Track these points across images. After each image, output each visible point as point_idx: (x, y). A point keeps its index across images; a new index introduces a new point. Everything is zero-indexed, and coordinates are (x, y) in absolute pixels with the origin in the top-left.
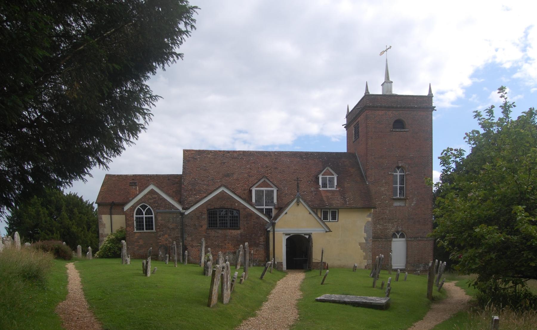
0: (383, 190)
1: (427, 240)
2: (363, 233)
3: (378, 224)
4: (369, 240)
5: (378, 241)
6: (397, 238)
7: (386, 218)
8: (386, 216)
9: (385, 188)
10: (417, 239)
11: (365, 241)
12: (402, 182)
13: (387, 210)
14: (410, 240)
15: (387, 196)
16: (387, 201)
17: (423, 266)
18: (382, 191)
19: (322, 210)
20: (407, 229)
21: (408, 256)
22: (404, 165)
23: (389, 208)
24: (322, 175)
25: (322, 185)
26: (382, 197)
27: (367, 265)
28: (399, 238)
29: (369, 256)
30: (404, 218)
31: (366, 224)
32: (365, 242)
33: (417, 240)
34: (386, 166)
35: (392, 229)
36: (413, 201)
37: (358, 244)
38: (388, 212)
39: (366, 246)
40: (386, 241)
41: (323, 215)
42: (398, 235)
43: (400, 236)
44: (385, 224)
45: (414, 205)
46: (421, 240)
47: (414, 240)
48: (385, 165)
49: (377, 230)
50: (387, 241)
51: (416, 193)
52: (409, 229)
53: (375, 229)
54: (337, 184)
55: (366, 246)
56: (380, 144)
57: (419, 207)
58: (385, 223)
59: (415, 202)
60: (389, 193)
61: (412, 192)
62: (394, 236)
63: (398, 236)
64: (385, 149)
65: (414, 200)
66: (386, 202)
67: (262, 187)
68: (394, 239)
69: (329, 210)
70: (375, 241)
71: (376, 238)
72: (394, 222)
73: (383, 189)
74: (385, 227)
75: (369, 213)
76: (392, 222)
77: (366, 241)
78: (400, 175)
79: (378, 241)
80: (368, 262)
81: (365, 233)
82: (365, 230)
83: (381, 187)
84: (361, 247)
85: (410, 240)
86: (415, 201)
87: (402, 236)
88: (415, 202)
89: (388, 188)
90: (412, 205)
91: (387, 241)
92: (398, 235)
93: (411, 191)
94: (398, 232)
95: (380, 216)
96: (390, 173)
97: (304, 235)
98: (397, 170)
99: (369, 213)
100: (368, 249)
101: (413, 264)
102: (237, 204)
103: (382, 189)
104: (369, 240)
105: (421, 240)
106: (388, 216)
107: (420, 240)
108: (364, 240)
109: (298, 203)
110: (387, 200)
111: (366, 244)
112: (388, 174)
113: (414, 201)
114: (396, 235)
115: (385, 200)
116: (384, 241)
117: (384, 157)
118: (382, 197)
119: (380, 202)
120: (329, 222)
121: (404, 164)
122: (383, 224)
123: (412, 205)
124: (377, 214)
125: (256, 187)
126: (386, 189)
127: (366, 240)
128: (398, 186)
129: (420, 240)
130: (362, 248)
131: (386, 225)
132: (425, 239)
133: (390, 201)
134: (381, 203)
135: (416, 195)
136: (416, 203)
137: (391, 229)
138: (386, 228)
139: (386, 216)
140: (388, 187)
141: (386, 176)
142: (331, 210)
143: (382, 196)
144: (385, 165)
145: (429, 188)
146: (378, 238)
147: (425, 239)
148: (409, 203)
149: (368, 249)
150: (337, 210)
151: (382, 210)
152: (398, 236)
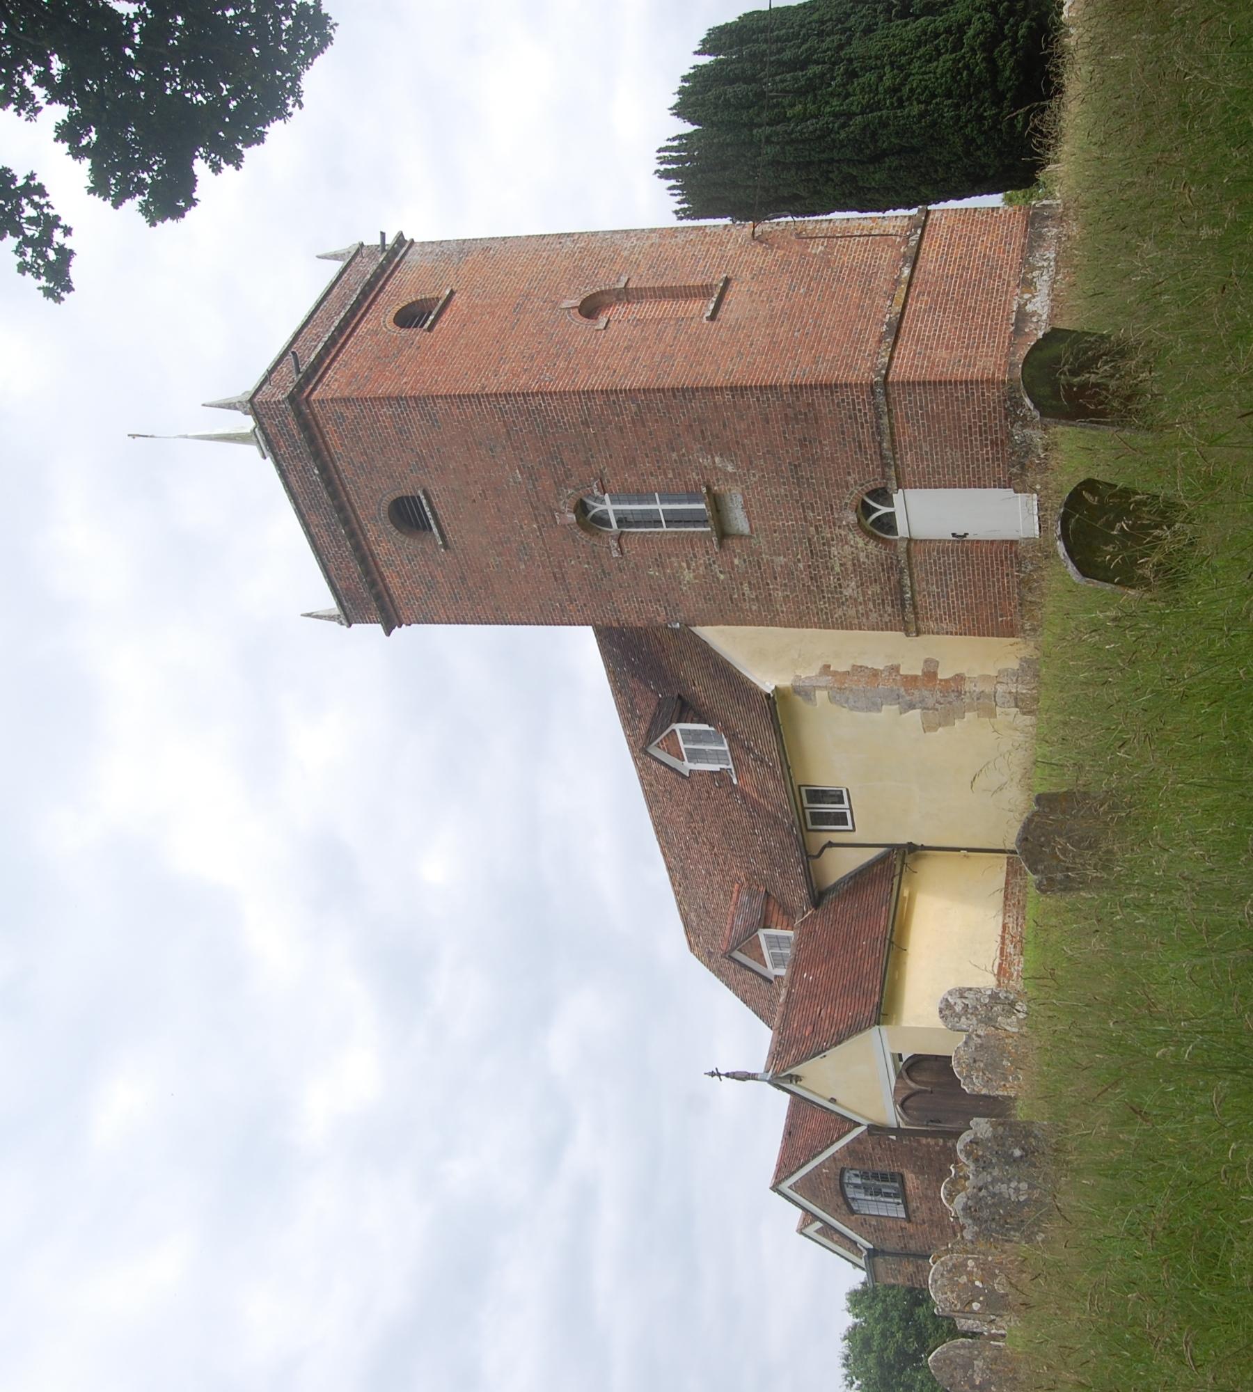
0: (691, 575)
1: (890, 410)
2: (879, 714)
3: (841, 593)
4: (908, 698)
5: (913, 597)
6: (893, 514)
7: (809, 566)
8: (801, 565)
9: (681, 567)
10: (889, 454)
11: (916, 713)
12: (641, 497)
13: (772, 561)
14: (894, 482)
15: (714, 562)
16: (736, 561)
17: (1023, 427)
18: (695, 578)
19: (810, 826)
20: (847, 488)
21: (976, 481)
22: (567, 501)
23: (761, 554)
24: (683, 760)
25: (719, 763)
26: (722, 577)
27: (1017, 706)
28: (893, 506)
29: (981, 701)
30: (797, 501)
31: (846, 705)
32: (918, 711)
33: (895, 453)
34: (588, 563)
35: (852, 543)
36: (715, 468)
37: (927, 733)
38: (782, 557)
39: (937, 710)
40: (910, 570)
41: (827, 824)
42: (878, 510)
43: (882, 505)
44: (837, 569)
45: (732, 461)
46: (892, 434)
47: (896, 466)
48: (586, 566)
49: (864, 596)
50: (909, 564)
51: (674, 455)
52: (847, 482)
53: (861, 604)
54: (705, 723)
55: (937, 710)
56: (511, 582)
57: (738, 443)
58: (832, 569)
59: (717, 459)
60: (699, 556)
61: (673, 470)
62: (887, 524)
63: (884, 510)
64: (523, 567)
65: (707, 462)
66: (737, 566)
67: (762, 955)
68: (902, 530)
69: (807, 812)
70: (915, 607)
71: (903, 606)
72: (823, 538)
73: (688, 576)
74: (851, 568)
75: (799, 699)
76: (824, 544)
77: (915, 709)
78: (613, 502)
79: (913, 597)
80: (1004, 703)
81: (879, 710)
82: (868, 709)
83: (680, 583)
84: (940, 725)
85: (898, 479)
86: (713, 457)
87: (882, 495)
88: (717, 459)
89: (678, 557)
90: (730, 469)
91: (909, 564)
92: (878, 510)
93: (670, 476)
94: (868, 510)
95: (804, 585)
96: (615, 554)
97: (901, 1060)
98: (596, 510)
99: (799, 699)
100: (950, 703)
101: (1014, 470)
102: (824, 1171)
103: (687, 578)
104: (908, 698)
105: (892, 434)
106: (799, 557)
107: (893, 441)
108: (912, 712)
109: (796, 1078)
110: (732, 563)
111: (928, 709)
112: (621, 558)
113: (714, 463)
114: (878, 518)
115: (733, 569)
116: (911, 576)
117: (556, 570)
118: (722, 577)
119: (742, 584)
120: (851, 808)
121: (562, 502)
122: (838, 574)
123: (730, 469)
124: (797, 596)
125: (766, 966)
126: (684, 565)
127: (912, 706)
128: (660, 507)
129: (893, 441)
130: (947, 720)
131: (841, 565)
132: (885, 420)
133: (734, 551)
134: (750, 583)
135: (684, 455)
136: (721, 455)
137: (857, 548)
138: (854, 565)
139: (801, 565)
140: (673, 559)
141: (632, 565)
142: (806, 804)
143: (718, 578)
144: (586, 566)
145: (638, 405)
146: (903, 600)
147: (885, 420)
148: (727, 480)
149: (950, 703)
150: (803, 789)
151: (776, 578)
152: (884, 510)
